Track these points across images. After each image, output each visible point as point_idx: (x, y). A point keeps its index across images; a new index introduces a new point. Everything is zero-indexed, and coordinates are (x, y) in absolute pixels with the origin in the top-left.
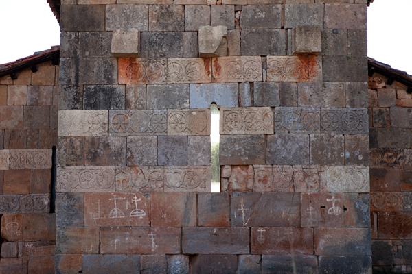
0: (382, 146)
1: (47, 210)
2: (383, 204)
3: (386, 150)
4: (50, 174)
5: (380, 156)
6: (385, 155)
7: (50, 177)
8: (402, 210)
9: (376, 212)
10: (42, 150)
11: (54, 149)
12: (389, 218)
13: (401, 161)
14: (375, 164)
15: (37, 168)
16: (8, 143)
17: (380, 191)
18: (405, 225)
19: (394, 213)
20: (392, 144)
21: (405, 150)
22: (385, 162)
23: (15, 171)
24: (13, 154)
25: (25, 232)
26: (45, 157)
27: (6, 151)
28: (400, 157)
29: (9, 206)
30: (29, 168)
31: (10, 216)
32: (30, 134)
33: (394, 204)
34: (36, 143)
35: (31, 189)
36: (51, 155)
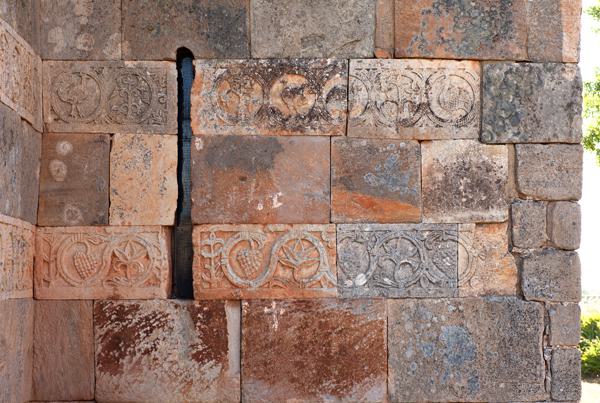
0: (265, 49)
2: (263, 271)
3: (281, 67)
5: (257, 87)
6: (277, 86)
8: (335, 292)
9: (237, 301)
12: (284, 326)
13: (336, 107)
14: (235, 120)
17: (252, 221)
18: (343, 349)
19: (305, 304)
20: (304, 42)
21: (353, 64)
22: (274, 112)
28: (334, 91)
33: (305, 272)
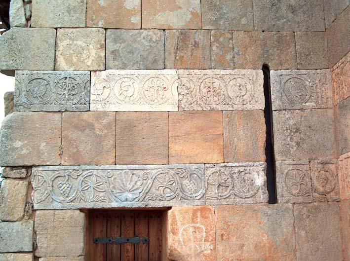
1: (263, 196)
4: (263, 120)
7: (264, 127)
10: (243, 72)
11: (266, 69)
15: (235, 107)
16: (173, 56)
23: (193, 113)
24: (184, 80)
25: (220, 247)
26: (249, 86)
27: (170, 73)
29: (182, 190)
30: (219, 108)
31: (187, 212)
32: (217, 41)
34: (229, 57)
35: (226, 152)
36: (262, 82)
